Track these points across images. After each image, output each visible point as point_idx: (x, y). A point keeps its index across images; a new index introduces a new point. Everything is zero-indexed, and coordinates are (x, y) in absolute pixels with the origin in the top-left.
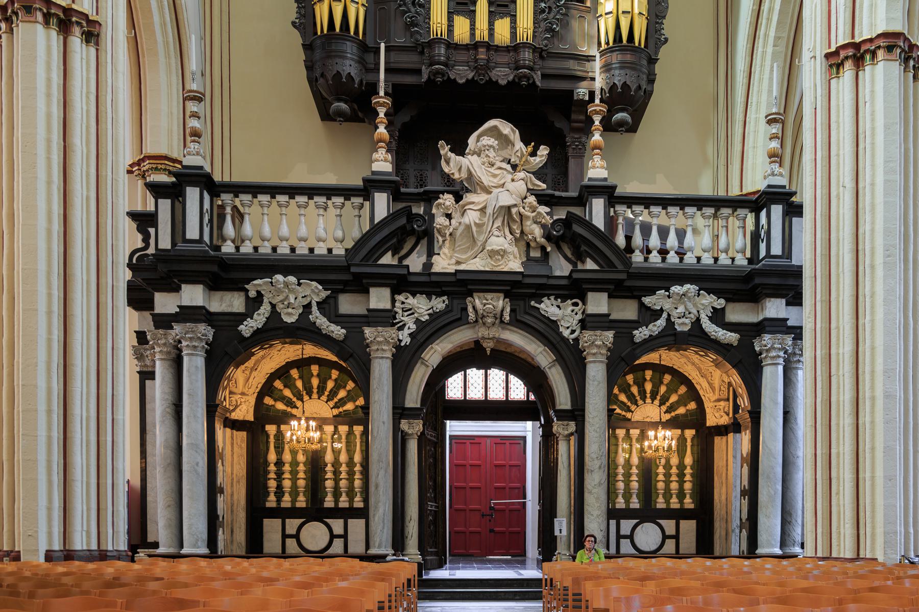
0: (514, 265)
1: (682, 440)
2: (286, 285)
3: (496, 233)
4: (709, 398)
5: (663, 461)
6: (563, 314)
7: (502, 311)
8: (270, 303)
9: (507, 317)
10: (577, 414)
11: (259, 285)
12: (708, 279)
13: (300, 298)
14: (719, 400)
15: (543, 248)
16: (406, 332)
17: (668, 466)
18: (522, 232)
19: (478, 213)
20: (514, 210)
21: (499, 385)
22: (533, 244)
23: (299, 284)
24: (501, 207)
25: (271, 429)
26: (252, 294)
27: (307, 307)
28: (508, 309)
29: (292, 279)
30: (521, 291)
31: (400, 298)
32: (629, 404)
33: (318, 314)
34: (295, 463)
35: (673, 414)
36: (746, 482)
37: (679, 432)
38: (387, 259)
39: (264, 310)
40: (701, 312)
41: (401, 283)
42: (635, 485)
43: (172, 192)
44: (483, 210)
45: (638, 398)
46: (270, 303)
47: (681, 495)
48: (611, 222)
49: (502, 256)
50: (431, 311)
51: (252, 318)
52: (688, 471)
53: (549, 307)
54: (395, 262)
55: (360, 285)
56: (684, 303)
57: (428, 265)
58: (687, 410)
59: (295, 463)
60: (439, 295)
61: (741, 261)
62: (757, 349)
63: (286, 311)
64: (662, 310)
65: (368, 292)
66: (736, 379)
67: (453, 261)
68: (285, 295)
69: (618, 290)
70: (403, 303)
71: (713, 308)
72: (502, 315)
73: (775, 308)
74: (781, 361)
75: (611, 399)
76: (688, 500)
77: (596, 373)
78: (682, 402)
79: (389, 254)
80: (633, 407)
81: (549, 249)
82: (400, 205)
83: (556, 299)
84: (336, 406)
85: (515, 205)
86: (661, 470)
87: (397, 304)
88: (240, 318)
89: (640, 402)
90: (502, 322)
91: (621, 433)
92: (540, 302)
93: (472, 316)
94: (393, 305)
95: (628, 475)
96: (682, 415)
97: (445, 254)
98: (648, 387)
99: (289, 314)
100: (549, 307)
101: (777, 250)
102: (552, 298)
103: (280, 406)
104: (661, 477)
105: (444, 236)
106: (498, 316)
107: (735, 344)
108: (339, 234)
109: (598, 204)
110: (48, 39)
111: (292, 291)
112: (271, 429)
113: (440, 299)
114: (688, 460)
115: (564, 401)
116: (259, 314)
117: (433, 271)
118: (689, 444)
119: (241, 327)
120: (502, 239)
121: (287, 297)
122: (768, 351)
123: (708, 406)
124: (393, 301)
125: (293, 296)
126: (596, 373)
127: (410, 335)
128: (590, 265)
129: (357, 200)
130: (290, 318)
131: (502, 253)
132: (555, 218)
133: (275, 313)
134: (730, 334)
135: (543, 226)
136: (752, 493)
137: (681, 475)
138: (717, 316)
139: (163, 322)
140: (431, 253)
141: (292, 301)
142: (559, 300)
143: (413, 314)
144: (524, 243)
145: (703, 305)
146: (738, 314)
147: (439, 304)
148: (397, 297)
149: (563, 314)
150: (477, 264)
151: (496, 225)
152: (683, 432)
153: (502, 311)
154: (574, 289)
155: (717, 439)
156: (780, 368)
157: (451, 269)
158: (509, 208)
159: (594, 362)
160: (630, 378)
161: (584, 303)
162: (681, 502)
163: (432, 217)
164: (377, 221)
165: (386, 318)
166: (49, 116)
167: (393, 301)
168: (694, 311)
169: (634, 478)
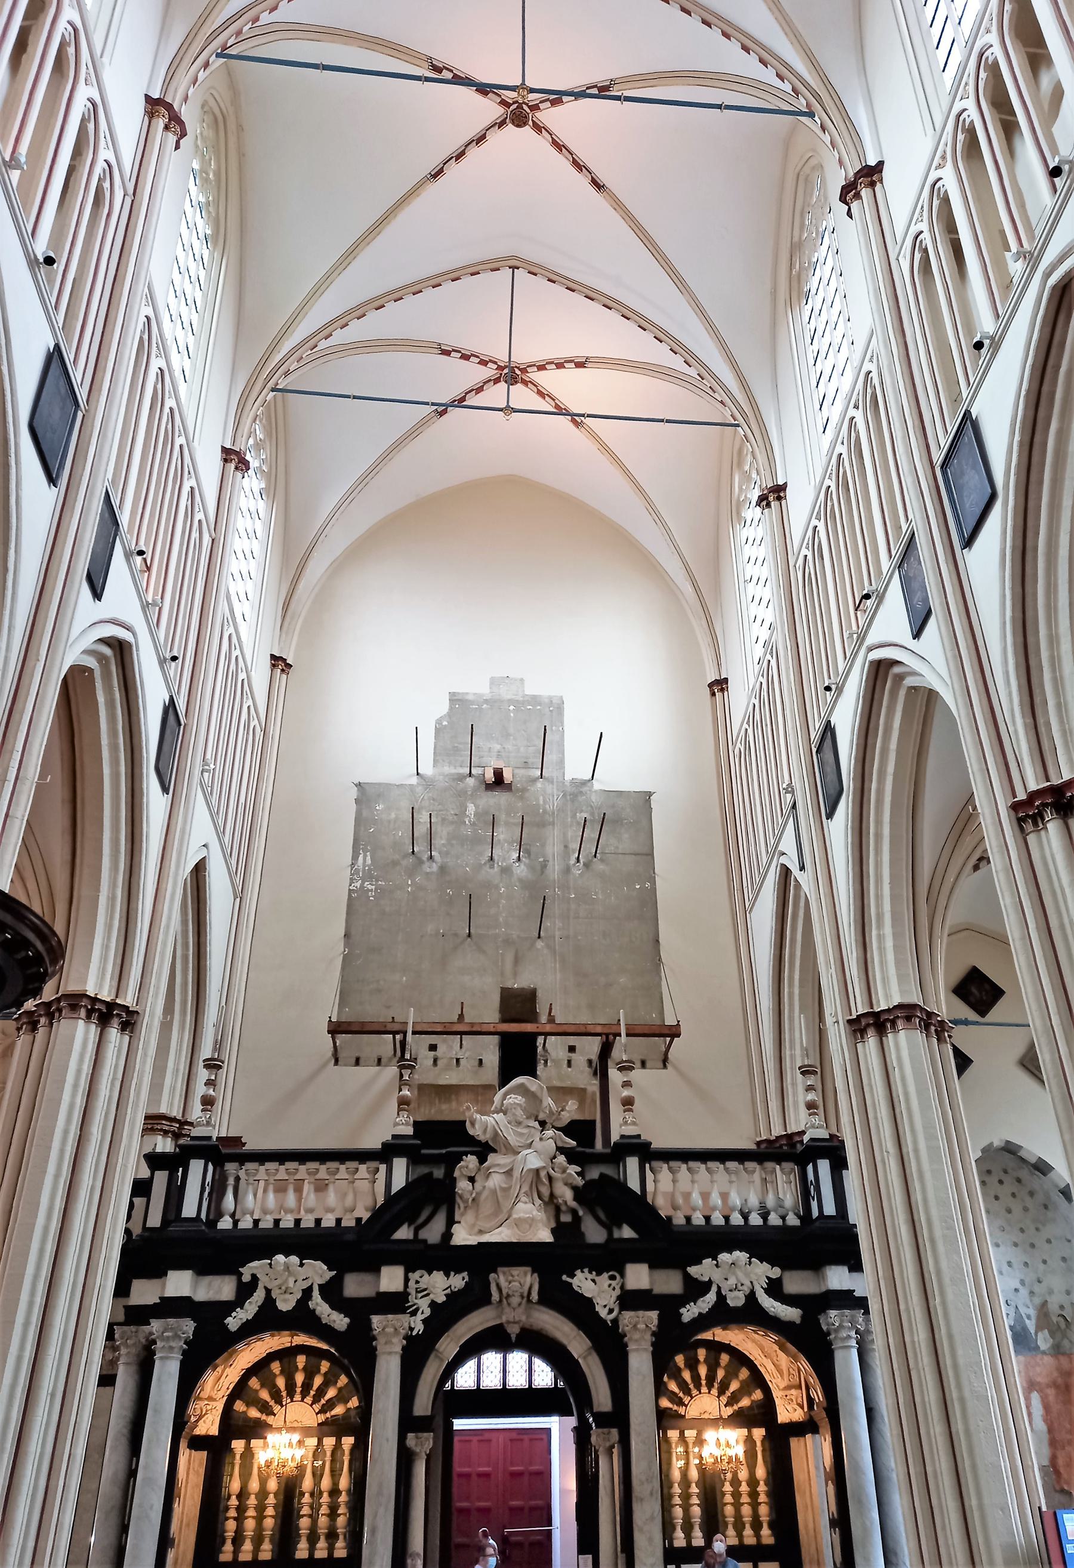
0: (544, 1235)
1: (749, 1441)
2: (287, 1267)
3: (524, 1199)
4: (776, 1384)
5: (729, 1476)
6: (596, 1288)
8: (265, 1288)
9: (535, 1296)
10: (619, 1418)
11: (256, 1268)
12: (760, 1242)
13: (300, 1281)
14: (788, 1388)
15: (574, 1212)
16: (420, 1317)
17: (736, 1482)
18: (552, 1195)
19: (503, 1177)
20: (543, 1174)
21: (522, 1370)
22: (563, 1208)
23: (302, 1265)
24: (530, 1170)
25: (238, 1445)
26: (246, 1278)
27: (307, 1293)
28: (536, 1287)
29: (294, 1259)
30: (552, 1263)
31: (414, 1276)
32: (681, 1395)
35: (736, 1407)
36: (833, 1508)
37: (745, 1431)
38: (404, 1233)
39: (259, 1296)
40: (755, 1283)
42: (696, 1511)
43: (170, 1163)
44: (509, 1173)
45: (691, 1386)
46: (265, 1288)
47: (757, 1525)
49: (530, 1226)
50: (448, 1291)
53: (583, 1282)
54: (411, 1236)
56: (734, 1274)
57: (448, 1235)
58: (753, 1401)
60: (458, 1271)
62: (825, 1328)
63: (282, 1297)
65: (377, 1271)
66: (804, 1364)
67: (476, 1230)
68: (284, 1278)
69: (656, 1264)
70: (417, 1282)
72: (529, 1293)
73: (837, 1278)
74: (853, 1343)
75: (660, 1389)
77: (640, 1364)
78: (745, 1390)
80: (686, 1400)
81: (581, 1213)
82: (423, 1170)
83: (590, 1272)
84: (322, 1411)
85: (544, 1167)
86: (728, 1488)
87: (412, 1284)
89: (694, 1392)
90: (529, 1301)
91: (673, 1434)
92: (573, 1276)
93: (495, 1296)
95: (686, 1496)
96: (750, 1408)
98: (703, 1371)
99: (285, 1301)
100: (583, 1282)
101: (830, 1209)
102: (586, 1270)
103: (254, 1413)
104: (728, 1498)
105: (466, 1201)
106: (525, 1294)
107: (798, 1321)
108: (349, 1201)
109: (632, 1164)
110: (87, 1032)
111: (290, 1274)
113: (459, 1277)
114: (761, 1472)
115: (602, 1398)
118: (759, 1449)
121: (286, 1281)
122: (837, 1331)
123: (777, 1394)
124: (407, 1280)
125: (289, 1278)
126: (640, 1364)
127: (424, 1321)
129: (373, 1164)
130: (285, 1304)
131: (531, 1222)
132: (588, 1178)
133: (269, 1301)
135: (575, 1188)
136: (842, 1522)
137: (754, 1494)
138: (774, 1288)
140: (451, 1222)
141: (291, 1284)
143: (428, 1295)
144: (553, 1206)
145: (756, 1274)
146: (797, 1283)
147: (458, 1281)
149: (596, 1288)
151: (523, 1191)
152: (749, 1432)
154: (609, 1260)
155: (794, 1442)
156: (854, 1353)
157: (473, 1240)
158: (537, 1171)
159: (637, 1350)
160: (680, 1359)
161: (622, 1276)
162: (757, 1535)
163: (454, 1181)
164: (394, 1191)
166: (71, 1106)
169: (695, 1500)
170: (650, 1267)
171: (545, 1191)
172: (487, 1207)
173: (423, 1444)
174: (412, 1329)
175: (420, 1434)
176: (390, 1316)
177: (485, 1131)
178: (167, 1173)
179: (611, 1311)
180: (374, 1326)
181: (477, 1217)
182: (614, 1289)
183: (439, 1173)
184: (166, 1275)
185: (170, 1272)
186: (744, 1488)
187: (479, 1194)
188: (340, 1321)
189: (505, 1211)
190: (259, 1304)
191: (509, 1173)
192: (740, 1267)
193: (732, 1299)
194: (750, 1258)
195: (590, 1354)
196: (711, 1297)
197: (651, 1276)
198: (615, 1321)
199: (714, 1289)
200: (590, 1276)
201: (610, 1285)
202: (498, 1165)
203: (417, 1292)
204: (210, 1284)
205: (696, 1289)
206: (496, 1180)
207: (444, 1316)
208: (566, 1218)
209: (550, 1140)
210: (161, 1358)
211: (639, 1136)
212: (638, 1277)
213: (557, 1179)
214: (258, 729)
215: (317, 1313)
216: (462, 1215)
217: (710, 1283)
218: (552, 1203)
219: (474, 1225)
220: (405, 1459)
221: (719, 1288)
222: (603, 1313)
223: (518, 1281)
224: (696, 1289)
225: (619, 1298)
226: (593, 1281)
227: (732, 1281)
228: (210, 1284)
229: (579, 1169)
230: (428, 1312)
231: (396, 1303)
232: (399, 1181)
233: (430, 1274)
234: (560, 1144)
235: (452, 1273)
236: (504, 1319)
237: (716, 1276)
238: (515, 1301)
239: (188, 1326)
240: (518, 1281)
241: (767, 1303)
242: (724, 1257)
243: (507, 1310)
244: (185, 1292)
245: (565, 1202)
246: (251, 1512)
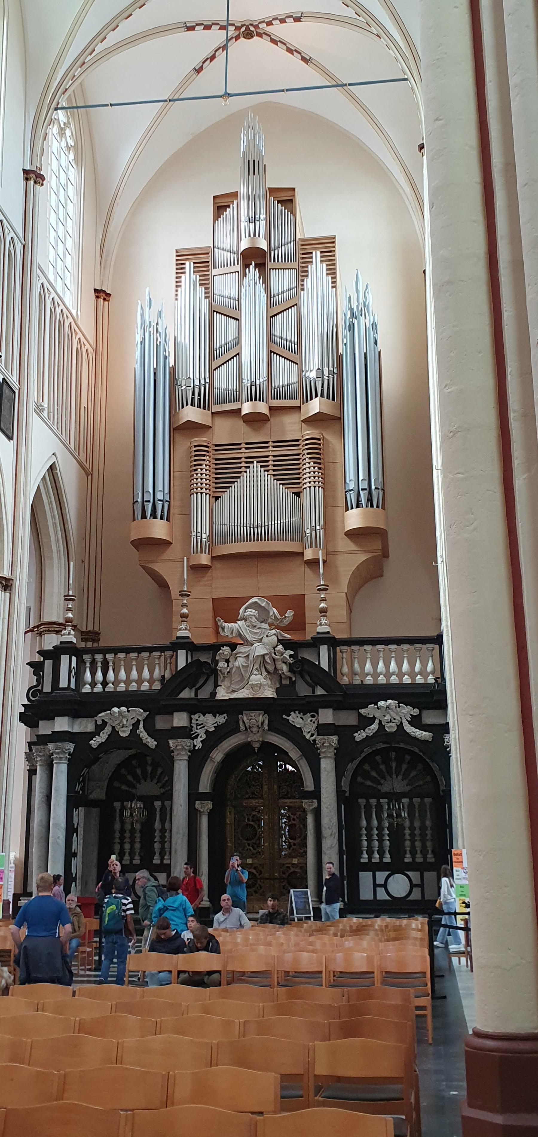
0: (269, 693)
7: (263, 723)
9: (266, 727)
16: (199, 739)
20: (267, 658)
22: (283, 676)
23: (128, 711)
24: (257, 656)
28: (266, 722)
29: (124, 709)
31: (195, 717)
33: (142, 730)
34: (133, 830)
38: (186, 694)
39: (108, 730)
41: (194, 707)
48: (333, 662)
49: (260, 688)
50: (216, 725)
51: (99, 736)
52: (429, 832)
53: (295, 719)
55: (169, 711)
56: (388, 713)
57: (214, 694)
59: (133, 830)
61: (431, 679)
64: (374, 718)
69: (338, 707)
70: (197, 720)
71: (411, 715)
76: (430, 856)
83: (299, 713)
87: (193, 721)
88: (91, 735)
92: (289, 715)
93: (242, 728)
94: (191, 723)
97: (225, 686)
100: (295, 719)
109: (324, 650)
111: (123, 717)
112: (117, 805)
116: (103, 733)
117: (216, 698)
119: (92, 742)
120: (259, 676)
121: (122, 721)
127: (202, 741)
128: (320, 691)
131: (260, 686)
134: (424, 733)
139: (41, 740)
140: (216, 685)
141: (125, 722)
143: (204, 727)
147: (221, 719)
148: (192, 716)
150: (244, 694)
151: (255, 668)
153: (263, 723)
154: (310, 707)
158: (263, 656)
165: (186, 733)
167: (191, 719)
168: (398, 718)
170: (334, 710)
171: (271, 668)
172: (236, 678)
173: (205, 807)
174: (195, 746)
175: (203, 802)
176: (179, 740)
177: (232, 633)
178: (51, 661)
179: (312, 735)
180: (171, 745)
181: (231, 683)
182: (314, 723)
183: (205, 658)
184: (54, 719)
185: (56, 718)
186: (417, 832)
187: (231, 669)
188: (152, 743)
189: (246, 679)
190: (108, 733)
192: (392, 709)
193: (388, 727)
194: (399, 703)
196: (375, 726)
197: (334, 715)
198: (314, 741)
199: (377, 721)
200: (299, 716)
201: (311, 721)
203: (197, 725)
204: (81, 723)
205: (366, 722)
206: (240, 661)
207: (214, 739)
208: (285, 682)
209: (272, 637)
210: (56, 763)
211: (328, 633)
212: (327, 716)
213: (278, 659)
214: (90, 350)
215: (141, 736)
216: (223, 681)
217: (374, 718)
218: (274, 674)
219: (229, 687)
220: (193, 815)
221: (380, 721)
222: (308, 737)
223: (255, 719)
224: (366, 722)
225: (317, 728)
226: (301, 718)
227: (388, 717)
228: (81, 723)
229: (292, 653)
230: (204, 736)
231: (186, 733)
232: (182, 663)
233: (204, 715)
234: (280, 638)
235: (218, 715)
236: (249, 740)
237: (378, 714)
238: (255, 729)
239: (71, 747)
240: (255, 719)
241: (409, 729)
242: (381, 703)
243: (251, 735)
244: (66, 728)
245: (283, 673)
246: (127, 840)
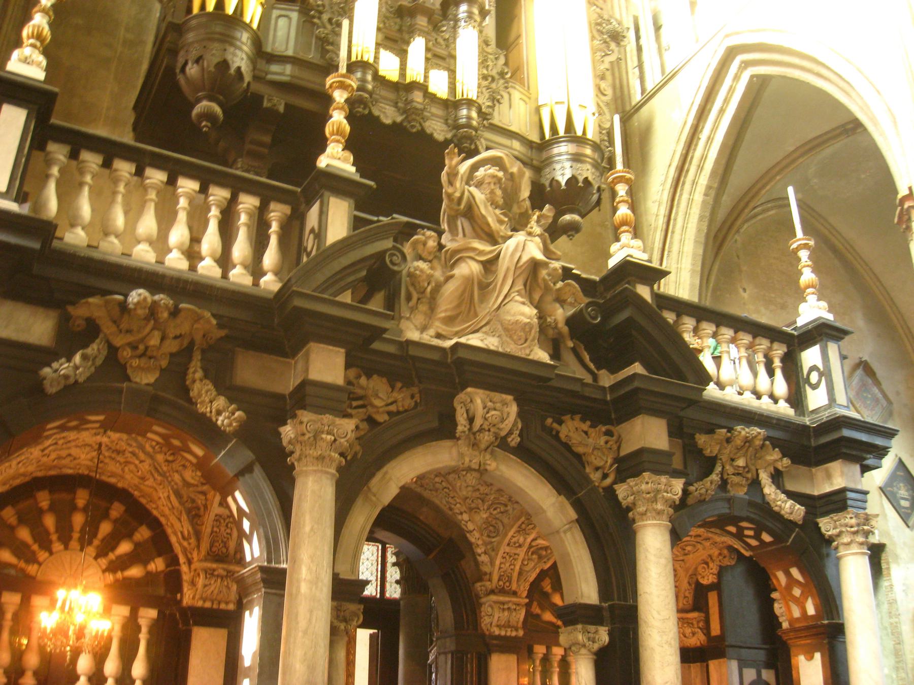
3: (518, 298)
50: (393, 408)
60: (408, 384)
79: (349, 292)
88: (46, 355)
92: (560, 423)
113: (406, 393)
142: (588, 423)
191: (490, 265)
195: (570, 529)
202: (474, 249)
222: (595, 477)
226: (586, 433)
